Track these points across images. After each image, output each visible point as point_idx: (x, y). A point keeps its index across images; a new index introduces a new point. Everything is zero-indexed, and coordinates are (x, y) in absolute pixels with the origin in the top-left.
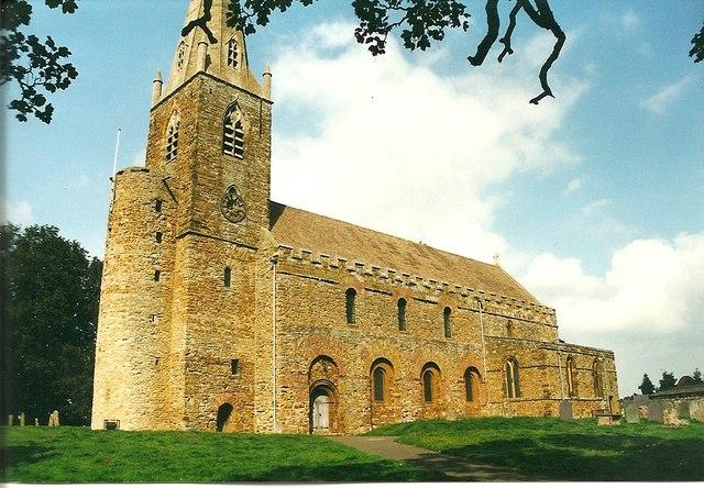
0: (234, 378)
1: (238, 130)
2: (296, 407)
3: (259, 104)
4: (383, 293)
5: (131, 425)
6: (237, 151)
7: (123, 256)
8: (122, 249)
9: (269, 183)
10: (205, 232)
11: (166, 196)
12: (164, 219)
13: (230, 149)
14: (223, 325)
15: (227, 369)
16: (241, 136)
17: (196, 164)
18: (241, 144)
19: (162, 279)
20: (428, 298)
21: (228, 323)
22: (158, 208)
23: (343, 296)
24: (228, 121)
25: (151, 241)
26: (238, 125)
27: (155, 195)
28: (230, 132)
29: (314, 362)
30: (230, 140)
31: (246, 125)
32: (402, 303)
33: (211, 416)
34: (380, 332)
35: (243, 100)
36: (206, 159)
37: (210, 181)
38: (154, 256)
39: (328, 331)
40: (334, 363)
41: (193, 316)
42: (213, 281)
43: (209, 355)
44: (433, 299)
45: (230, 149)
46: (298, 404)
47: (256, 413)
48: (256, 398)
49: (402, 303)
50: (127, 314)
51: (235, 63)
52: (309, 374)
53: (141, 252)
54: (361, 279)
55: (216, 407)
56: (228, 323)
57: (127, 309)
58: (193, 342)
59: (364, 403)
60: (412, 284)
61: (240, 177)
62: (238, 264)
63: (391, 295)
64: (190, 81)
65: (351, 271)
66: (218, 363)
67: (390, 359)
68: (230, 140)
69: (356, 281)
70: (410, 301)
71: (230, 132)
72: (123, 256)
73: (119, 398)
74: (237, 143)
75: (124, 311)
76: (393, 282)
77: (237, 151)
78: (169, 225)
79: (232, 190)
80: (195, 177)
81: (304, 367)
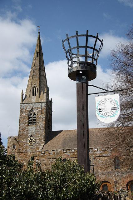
1: (34, 116)
11: (16, 143)
13: (31, 123)
16: (35, 117)
18: (35, 120)
20: (105, 155)
22: (14, 147)
24: (31, 114)
26: (35, 114)
28: (31, 118)
30: (31, 120)
31: (36, 113)
35: (35, 106)
36: (23, 130)
37: (24, 136)
44: (106, 155)
45: (31, 123)
61: (34, 131)
68: (31, 120)
71: (31, 118)
74: (34, 120)
79: (31, 136)
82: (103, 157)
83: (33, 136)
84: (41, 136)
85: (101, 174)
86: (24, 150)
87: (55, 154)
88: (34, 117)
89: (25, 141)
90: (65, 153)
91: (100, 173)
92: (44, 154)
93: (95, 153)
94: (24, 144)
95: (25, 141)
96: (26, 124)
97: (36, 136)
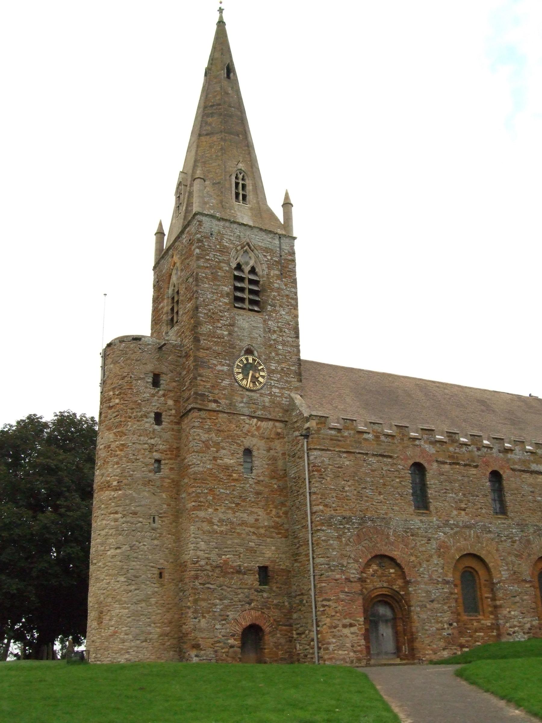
0: (262, 591)
1: (252, 277)
2: (345, 626)
3: (277, 242)
4: (465, 465)
5: (127, 656)
6: (252, 302)
7: (113, 446)
8: (111, 436)
9: (297, 337)
10: (213, 406)
12: (164, 395)
13: (242, 300)
14: (243, 523)
15: (252, 580)
17: (197, 324)
18: (256, 293)
19: (165, 471)
21: (251, 520)
22: (156, 383)
23: (407, 474)
25: (149, 423)
26: (253, 271)
27: (150, 367)
29: (368, 565)
31: (262, 270)
32: (496, 476)
33: (231, 641)
34: (464, 518)
37: (217, 343)
38: (152, 441)
39: (386, 521)
40: (398, 565)
41: (202, 514)
42: (227, 467)
43: (226, 562)
45: (242, 300)
46: (347, 621)
47: (295, 636)
48: (295, 616)
49: (496, 476)
50: (119, 515)
51: (244, 197)
52: (362, 580)
53: (135, 438)
54: (431, 449)
55: (239, 630)
56: (251, 520)
57: (120, 509)
58: (202, 545)
59: (447, 617)
60: (507, 451)
62: (262, 444)
63: (476, 467)
64: (188, 225)
65: (415, 439)
66: (239, 572)
67: (483, 554)
68: (242, 290)
69: (423, 451)
70: (506, 474)
72: (113, 446)
73: (113, 623)
74: (251, 292)
75: (116, 513)
76: (479, 449)
77: (252, 302)
78: (170, 402)
80: (196, 340)
81: (353, 573)
82: (532, 472)
83: (256, 353)
84: (285, 360)
85: (535, 532)
86: (223, 401)
87: (383, 438)
88: (251, 282)
89: (225, 368)
90: (417, 442)
91: (531, 530)
92: (339, 430)
93: (509, 455)
94: (220, 375)
95: (225, 368)
96: (226, 300)
97: (268, 359)
